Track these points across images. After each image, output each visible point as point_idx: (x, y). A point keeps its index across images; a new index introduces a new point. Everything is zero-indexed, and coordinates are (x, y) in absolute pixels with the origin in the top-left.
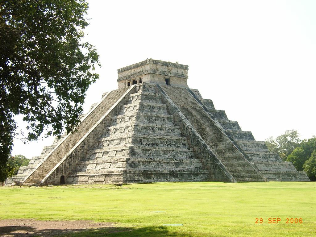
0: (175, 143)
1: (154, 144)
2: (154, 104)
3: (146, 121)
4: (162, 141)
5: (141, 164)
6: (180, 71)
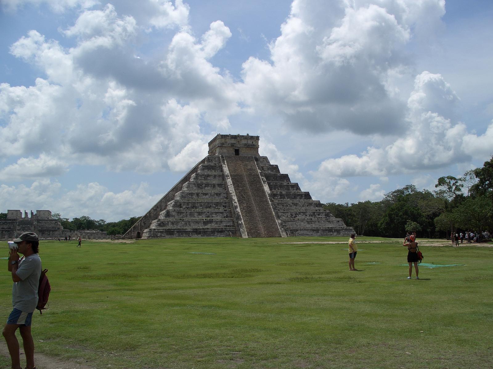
0: (215, 206)
1: (194, 207)
2: (210, 174)
3: (195, 188)
4: (202, 205)
5: (170, 223)
6: (250, 142)
